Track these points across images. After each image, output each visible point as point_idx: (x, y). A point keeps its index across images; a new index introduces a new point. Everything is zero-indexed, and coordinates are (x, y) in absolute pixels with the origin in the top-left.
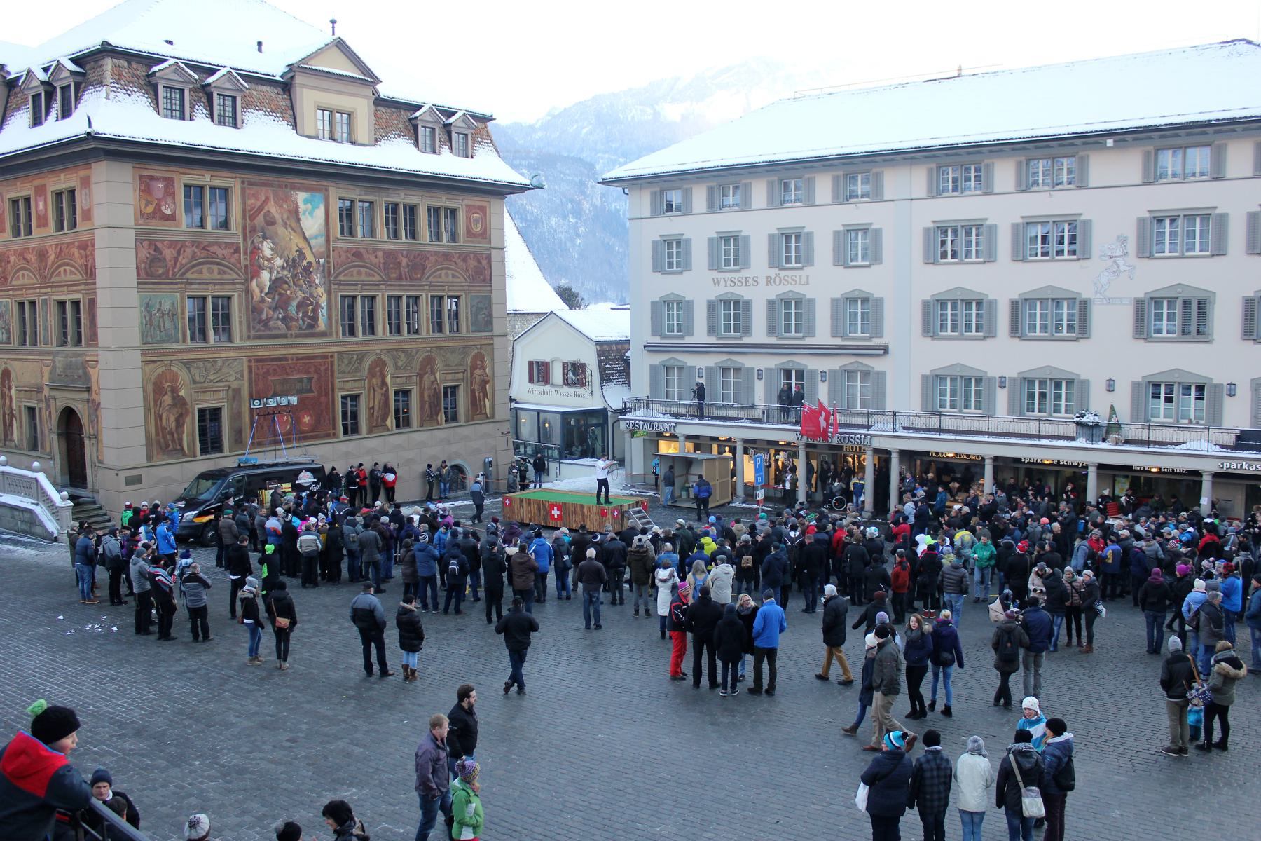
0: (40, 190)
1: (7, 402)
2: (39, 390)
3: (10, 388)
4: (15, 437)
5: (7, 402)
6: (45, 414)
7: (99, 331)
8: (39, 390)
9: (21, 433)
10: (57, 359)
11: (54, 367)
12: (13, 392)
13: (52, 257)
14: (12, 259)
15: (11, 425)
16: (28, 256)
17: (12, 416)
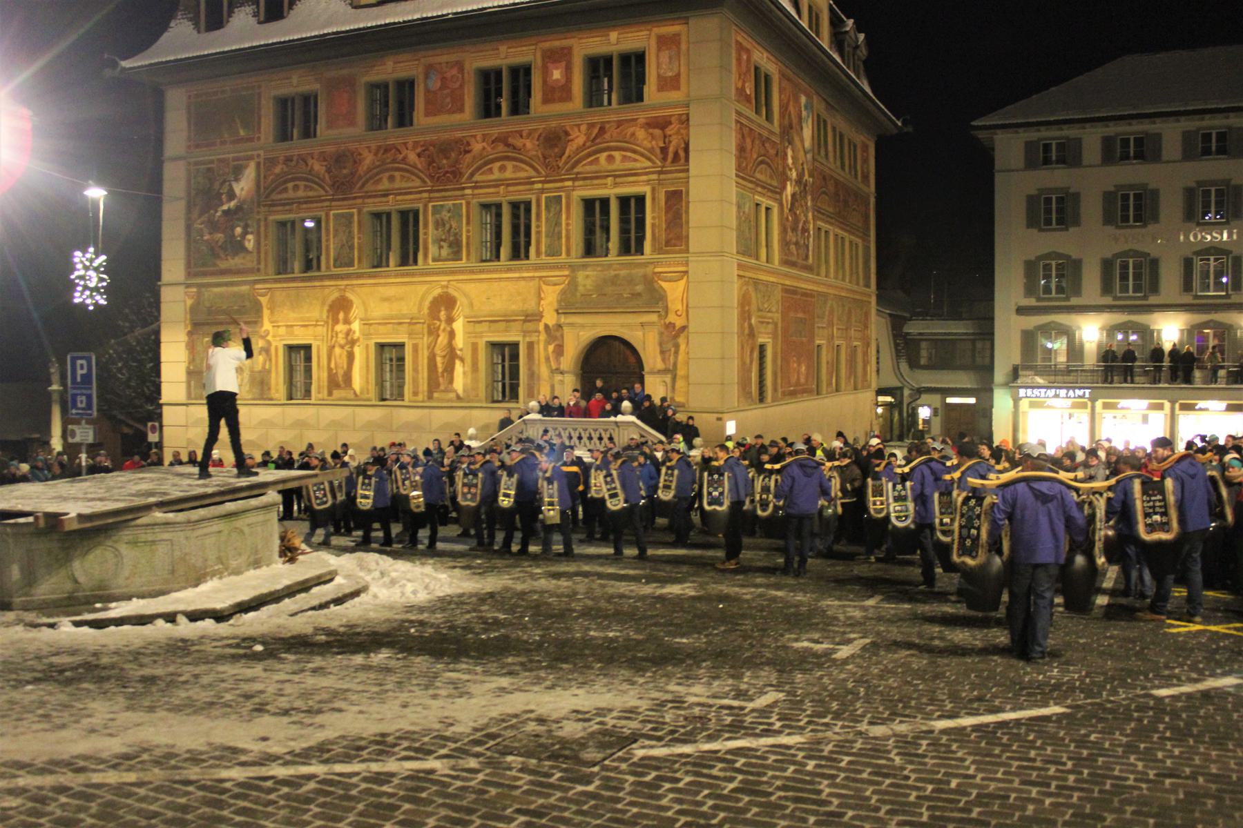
0: (562, 56)
1: (443, 339)
2: (532, 317)
3: (450, 320)
4: (459, 383)
5: (443, 339)
6: (543, 349)
7: (692, 234)
8: (538, 316)
9: (475, 380)
10: (581, 275)
11: (573, 283)
12: (459, 326)
13: (581, 140)
14: (477, 147)
15: (450, 369)
16: (518, 142)
17: (452, 355)
